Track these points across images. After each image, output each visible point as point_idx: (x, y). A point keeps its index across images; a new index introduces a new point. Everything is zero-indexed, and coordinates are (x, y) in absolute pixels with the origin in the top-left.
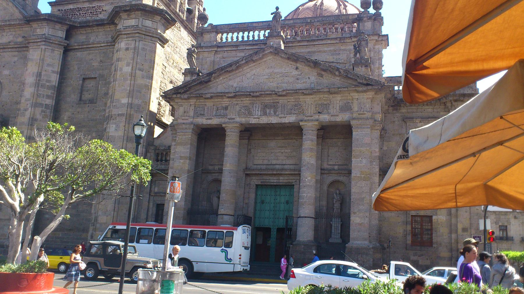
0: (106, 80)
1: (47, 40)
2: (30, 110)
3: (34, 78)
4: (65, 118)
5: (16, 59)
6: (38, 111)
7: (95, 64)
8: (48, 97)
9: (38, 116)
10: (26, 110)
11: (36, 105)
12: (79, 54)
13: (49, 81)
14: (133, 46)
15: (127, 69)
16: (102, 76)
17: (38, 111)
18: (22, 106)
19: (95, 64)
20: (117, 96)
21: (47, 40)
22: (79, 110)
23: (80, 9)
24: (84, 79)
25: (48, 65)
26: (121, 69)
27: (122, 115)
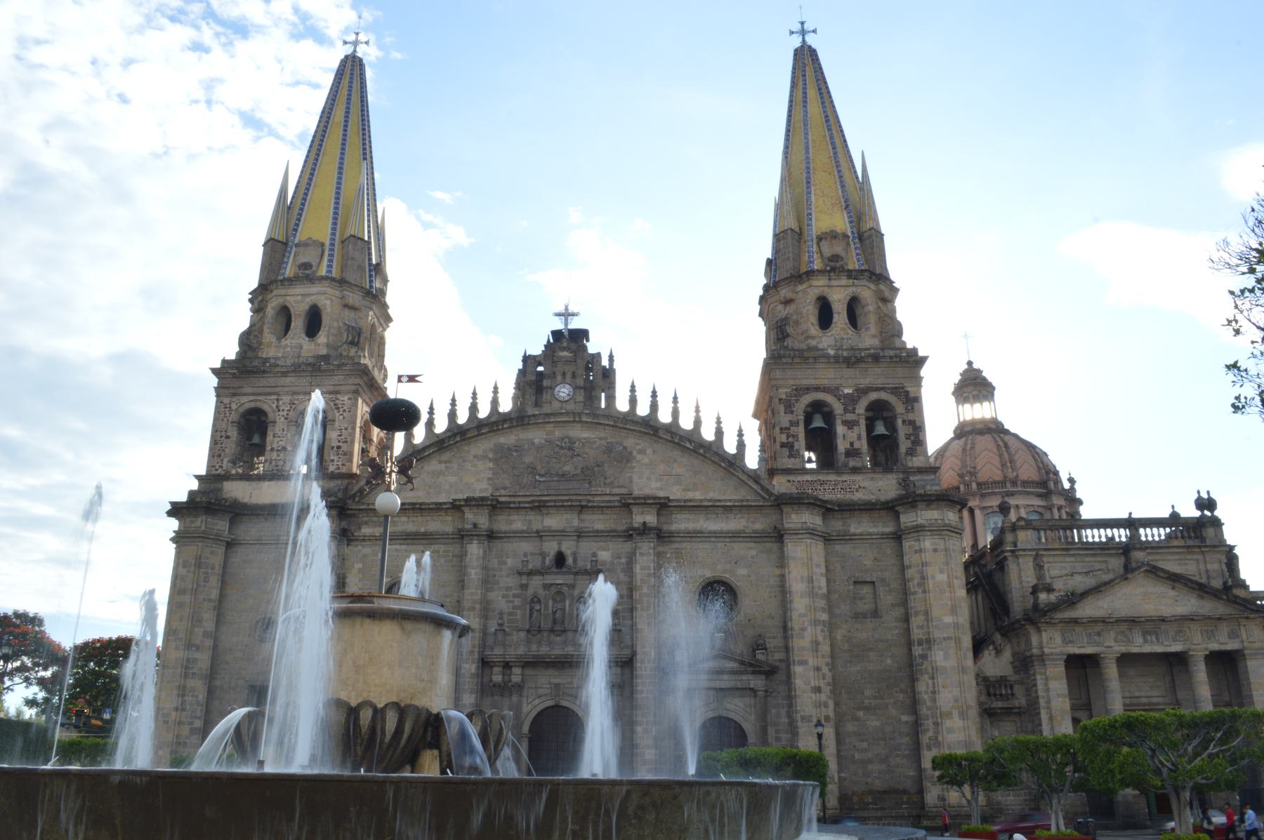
0: (889, 585)
1: (812, 533)
2: (809, 630)
3: (805, 584)
4: (839, 637)
5: (754, 552)
6: (819, 628)
7: (868, 563)
8: (823, 610)
9: (820, 639)
10: (803, 629)
11: (816, 622)
12: (838, 547)
13: (820, 588)
14: (942, 547)
15: (942, 578)
16: (883, 580)
17: (819, 628)
18: (796, 622)
19: (868, 563)
20: (935, 612)
21: (812, 533)
22: (858, 626)
23: (822, 483)
24: (855, 583)
25: (818, 566)
26: (933, 578)
27: (949, 638)
